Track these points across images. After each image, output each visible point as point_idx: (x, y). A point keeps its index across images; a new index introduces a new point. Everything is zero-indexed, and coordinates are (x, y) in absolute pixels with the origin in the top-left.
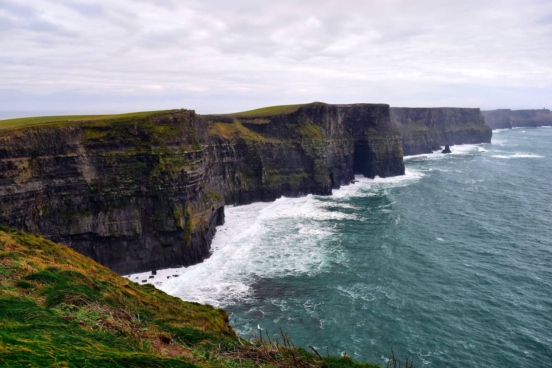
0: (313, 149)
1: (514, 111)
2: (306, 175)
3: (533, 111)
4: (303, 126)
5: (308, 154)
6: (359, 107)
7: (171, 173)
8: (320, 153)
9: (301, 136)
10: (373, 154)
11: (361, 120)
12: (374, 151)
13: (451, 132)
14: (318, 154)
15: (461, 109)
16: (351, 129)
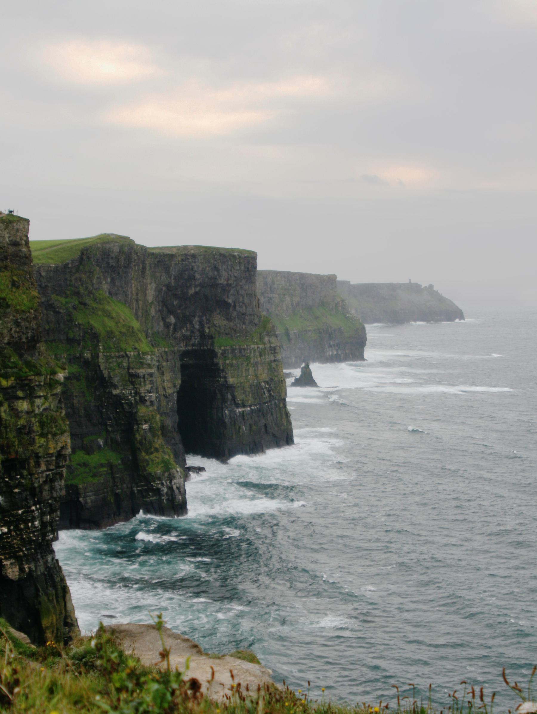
0: (131, 375)
1: (355, 287)
2: (115, 459)
3: (393, 288)
4: (94, 305)
5: (115, 392)
6: (194, 256)
7: (32, 463)
8: (148, 387)
9: (95, 337)
10: (230, 388)
11: (196, 293)
12: (231, 380)
13: (287, 334)
14: (142, 390)
15: (302, 276)
16: (172, 319)
